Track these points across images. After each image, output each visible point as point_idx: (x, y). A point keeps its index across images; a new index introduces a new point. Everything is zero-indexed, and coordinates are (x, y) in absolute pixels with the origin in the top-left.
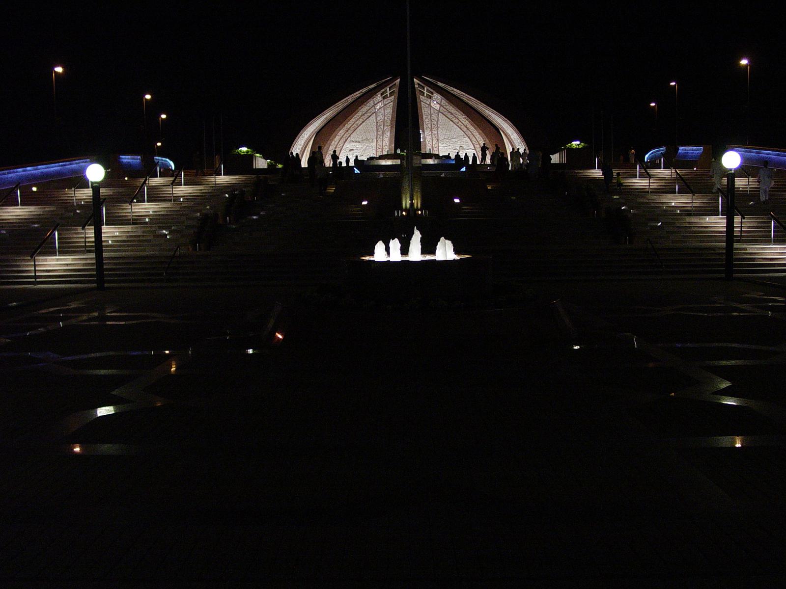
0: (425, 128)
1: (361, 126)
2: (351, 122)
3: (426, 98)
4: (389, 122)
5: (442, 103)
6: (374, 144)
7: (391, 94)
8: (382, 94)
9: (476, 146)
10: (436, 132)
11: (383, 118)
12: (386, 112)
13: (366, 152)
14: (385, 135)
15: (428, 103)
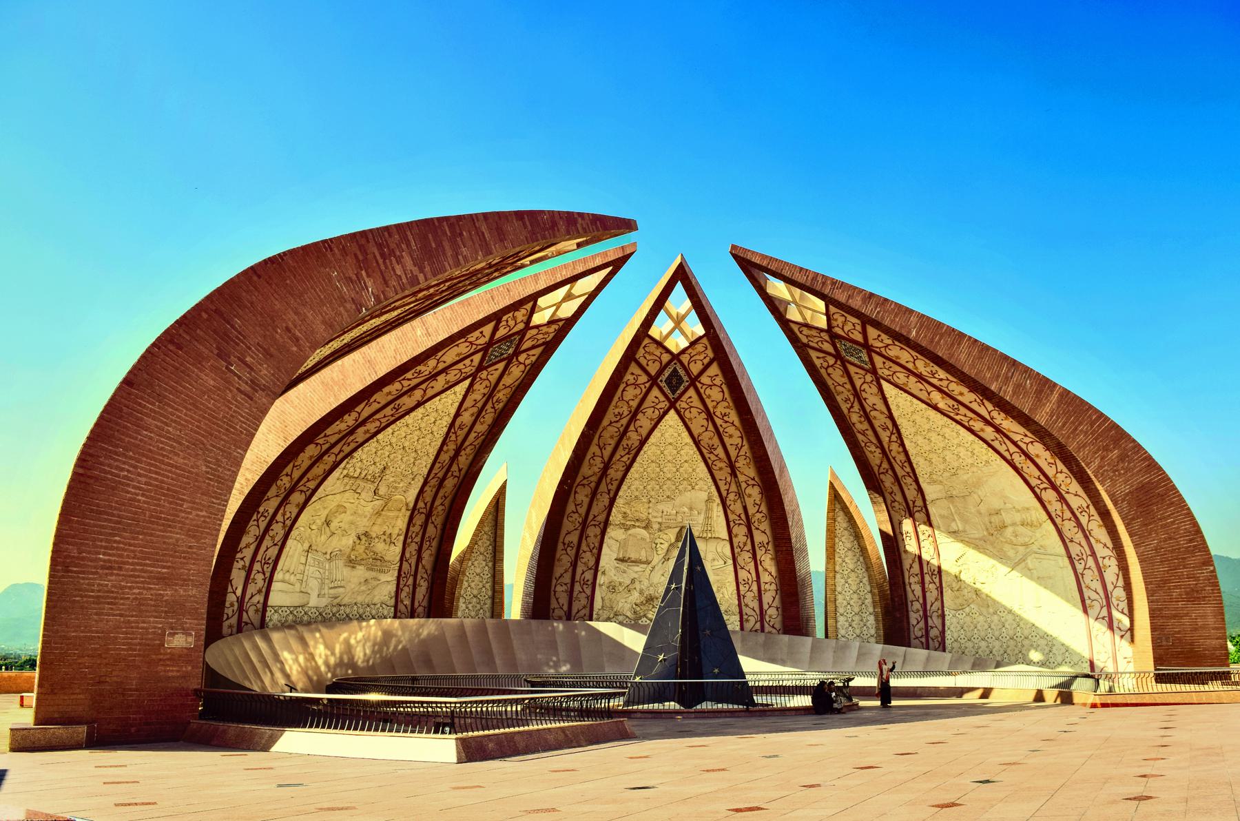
9: (735, 530)
10: (620, 474)
14: (455, 468)
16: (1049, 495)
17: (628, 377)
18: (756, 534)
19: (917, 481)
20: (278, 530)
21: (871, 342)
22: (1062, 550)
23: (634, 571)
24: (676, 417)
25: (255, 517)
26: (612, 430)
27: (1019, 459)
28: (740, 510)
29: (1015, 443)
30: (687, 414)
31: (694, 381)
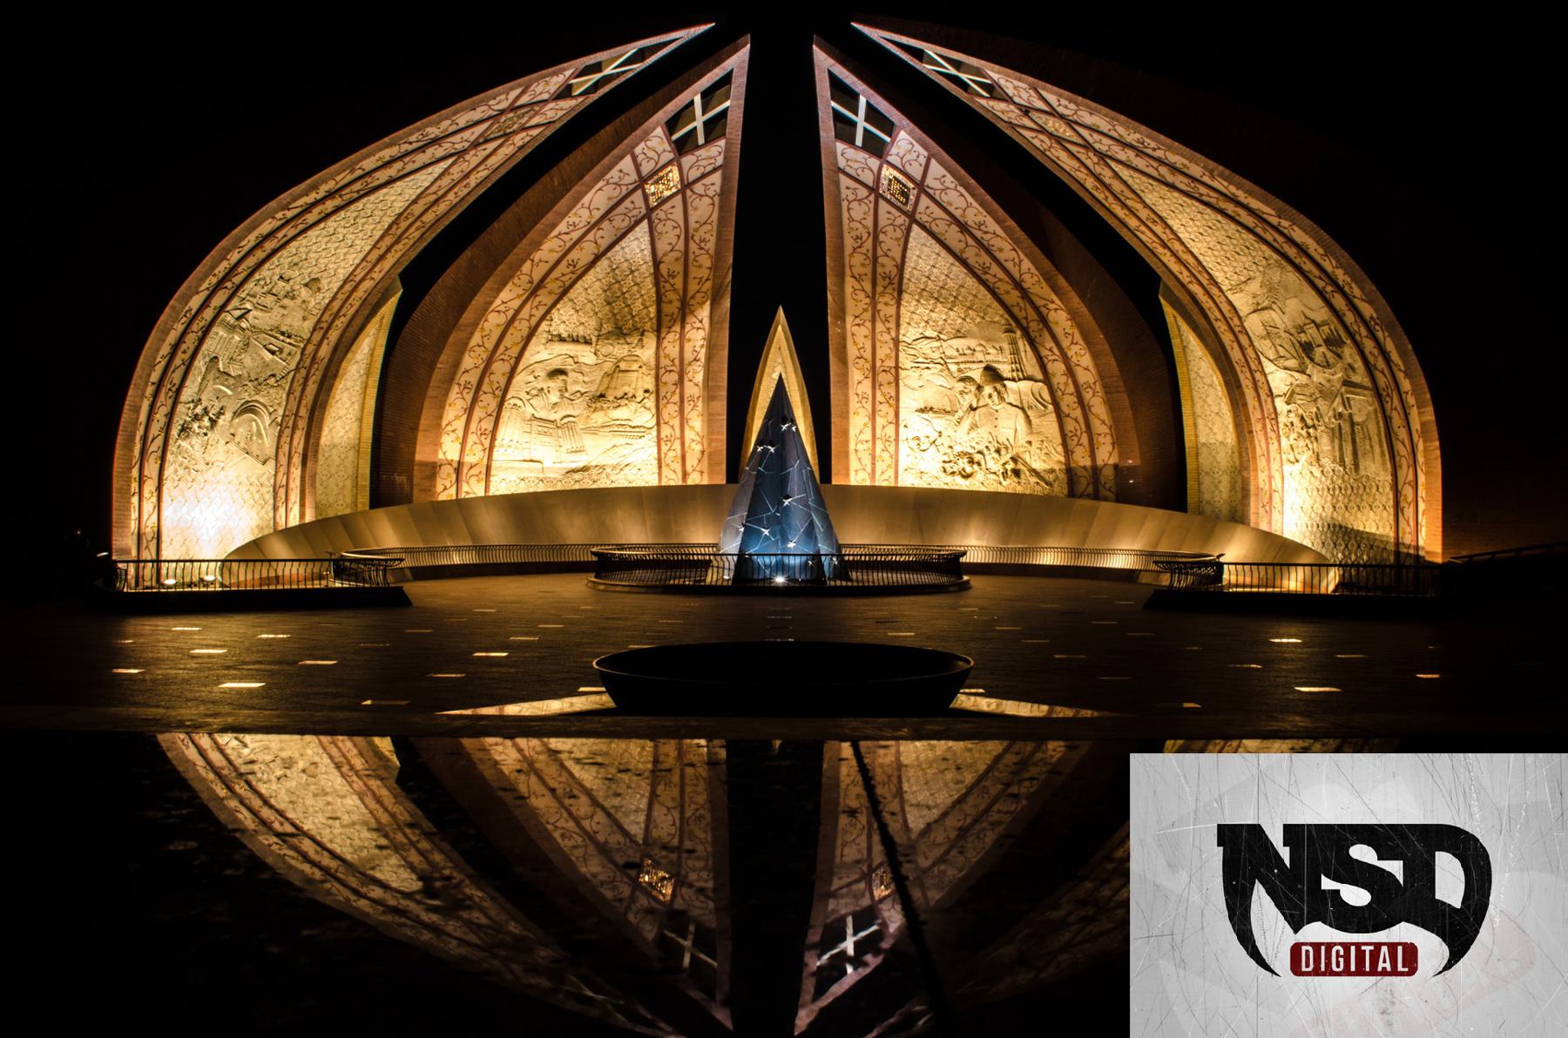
0: (848, 290)
1: (592, 272)
2: (548, 250)
3: (862, 156)
4: (706, 261)
5: (929, 181)
6: (647, 352)
7: (715, 127)
8: (671, 125)
9: (1051, 367)
10: (892, 310)
11: (681, 245)
12: (692, 218)
13: (613, 384)
14: (690, 319)
15: (869, 180)
16: (1339, 302)
17: (844, 193)
18: (1079, 372)
19: (1221, 290)
20: (488, 401)
21: (1060, 110)
22: (1367, 382)
23: (940, 423)
24: (924, 234)
25: (455, 389)
26: (858, 259)
27: (1292, 252)
28: (1050, 344)
29: (1275, 228)
30: (934, 228)
31: (921, 186)
